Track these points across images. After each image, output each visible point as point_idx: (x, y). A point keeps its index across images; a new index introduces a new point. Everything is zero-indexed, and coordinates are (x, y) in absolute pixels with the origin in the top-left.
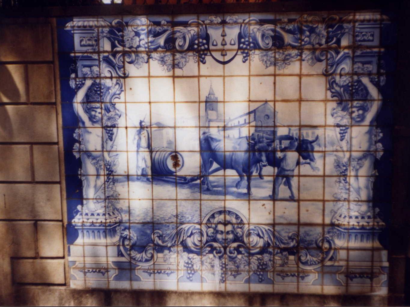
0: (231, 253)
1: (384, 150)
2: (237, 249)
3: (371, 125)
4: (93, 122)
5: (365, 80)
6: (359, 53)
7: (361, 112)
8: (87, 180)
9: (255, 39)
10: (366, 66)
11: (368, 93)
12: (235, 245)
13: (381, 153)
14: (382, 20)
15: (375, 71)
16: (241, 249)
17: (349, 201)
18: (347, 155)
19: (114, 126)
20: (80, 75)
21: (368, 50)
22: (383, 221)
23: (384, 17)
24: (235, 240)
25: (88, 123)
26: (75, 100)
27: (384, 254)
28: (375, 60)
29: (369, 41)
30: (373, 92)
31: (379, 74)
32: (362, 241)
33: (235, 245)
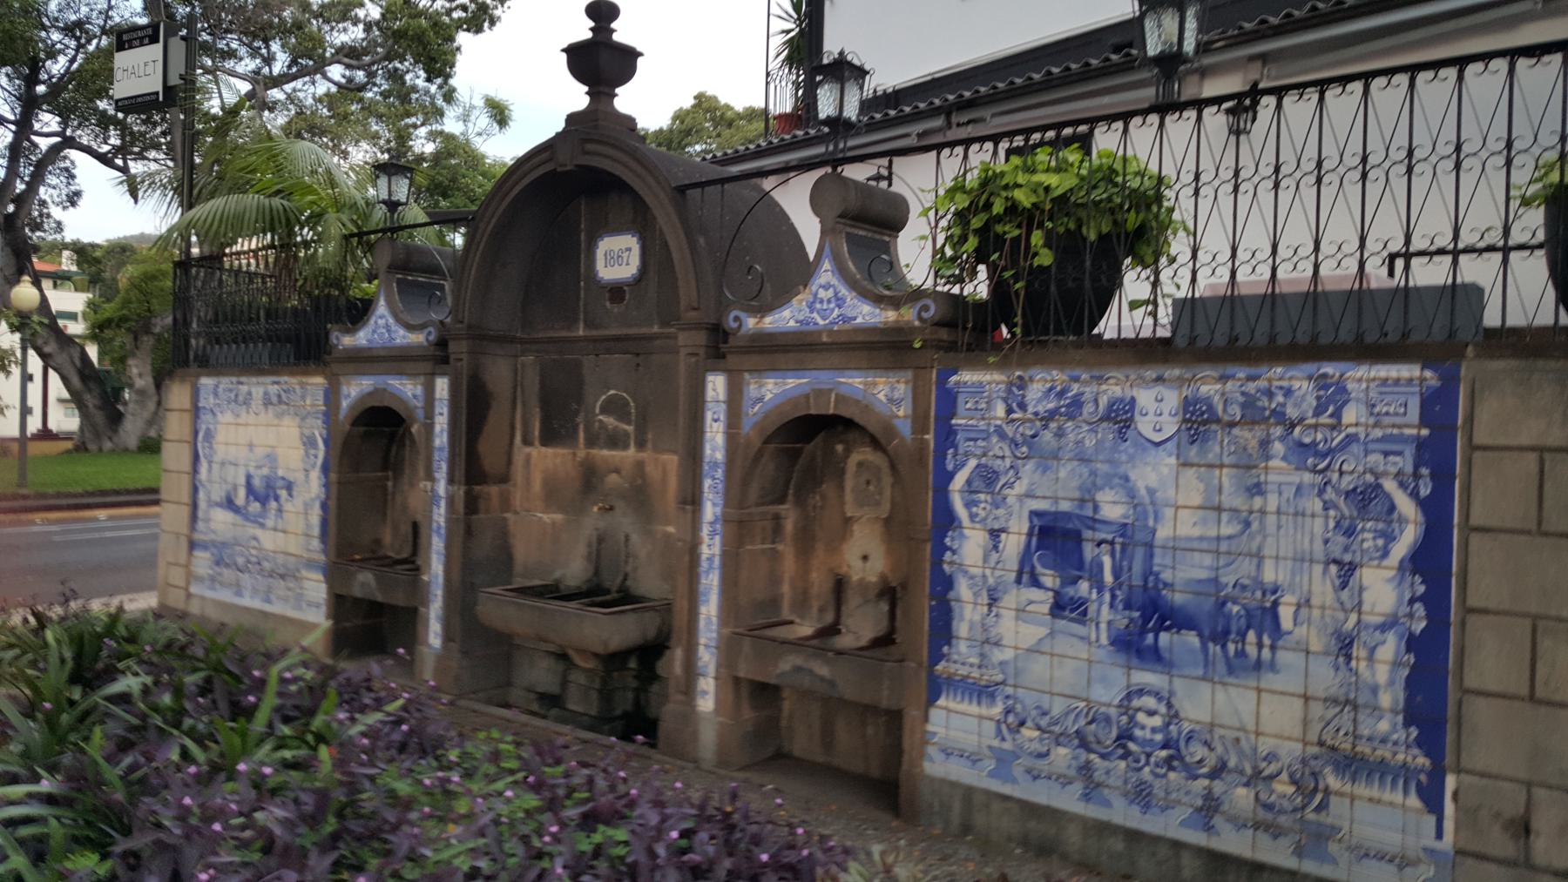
0: (1157, 765)
1: (1428, 616)
2: (1168, 762)
3: (1401, 567)
4: (972, 521)
5: (1389, 485)
6: (1378, 433)
7: (1380, 542)
8: (962, 608)
9: (1211, 408)
10: (1391, 458)
11: (1392, 508)
12: (1164, 753)
13: (1423, 624)
14: (1422, 380)
15: (1409, 469)
16: (1176, 763)
17: (1355, 708)
18: (1353, 618)
19: (1003, 530)
20: (961, 451)
21: (1395, 431)
22: (1427, 755)
23: (1428, 374)
24: (1165, 746)
25: (965, 521)
26: (951, 487)
27: (706, 646)
28: (1409, 452)
29: (1396, 414)
30: (1406, 506)
31: (1416, 476)
32: (979, 703)
33: (1164, 753)
